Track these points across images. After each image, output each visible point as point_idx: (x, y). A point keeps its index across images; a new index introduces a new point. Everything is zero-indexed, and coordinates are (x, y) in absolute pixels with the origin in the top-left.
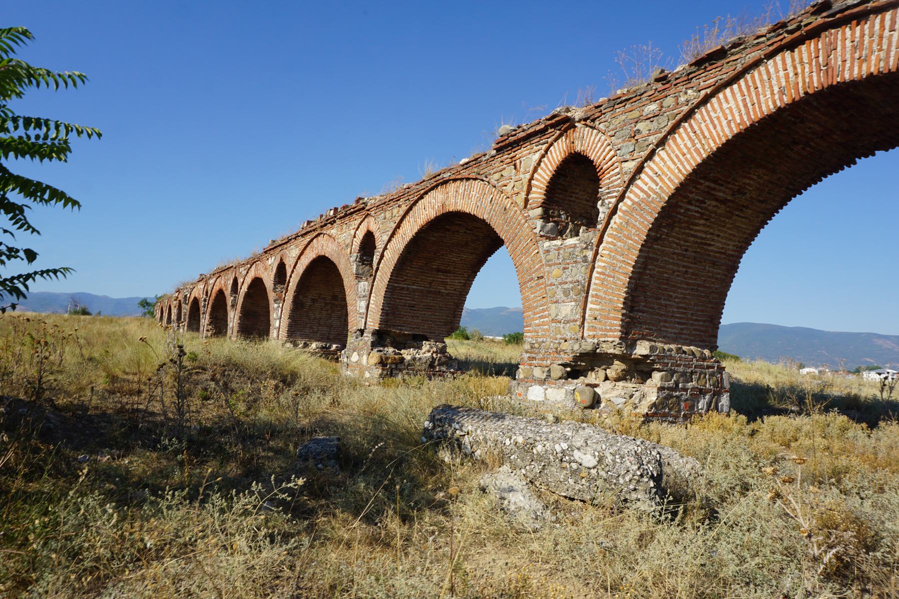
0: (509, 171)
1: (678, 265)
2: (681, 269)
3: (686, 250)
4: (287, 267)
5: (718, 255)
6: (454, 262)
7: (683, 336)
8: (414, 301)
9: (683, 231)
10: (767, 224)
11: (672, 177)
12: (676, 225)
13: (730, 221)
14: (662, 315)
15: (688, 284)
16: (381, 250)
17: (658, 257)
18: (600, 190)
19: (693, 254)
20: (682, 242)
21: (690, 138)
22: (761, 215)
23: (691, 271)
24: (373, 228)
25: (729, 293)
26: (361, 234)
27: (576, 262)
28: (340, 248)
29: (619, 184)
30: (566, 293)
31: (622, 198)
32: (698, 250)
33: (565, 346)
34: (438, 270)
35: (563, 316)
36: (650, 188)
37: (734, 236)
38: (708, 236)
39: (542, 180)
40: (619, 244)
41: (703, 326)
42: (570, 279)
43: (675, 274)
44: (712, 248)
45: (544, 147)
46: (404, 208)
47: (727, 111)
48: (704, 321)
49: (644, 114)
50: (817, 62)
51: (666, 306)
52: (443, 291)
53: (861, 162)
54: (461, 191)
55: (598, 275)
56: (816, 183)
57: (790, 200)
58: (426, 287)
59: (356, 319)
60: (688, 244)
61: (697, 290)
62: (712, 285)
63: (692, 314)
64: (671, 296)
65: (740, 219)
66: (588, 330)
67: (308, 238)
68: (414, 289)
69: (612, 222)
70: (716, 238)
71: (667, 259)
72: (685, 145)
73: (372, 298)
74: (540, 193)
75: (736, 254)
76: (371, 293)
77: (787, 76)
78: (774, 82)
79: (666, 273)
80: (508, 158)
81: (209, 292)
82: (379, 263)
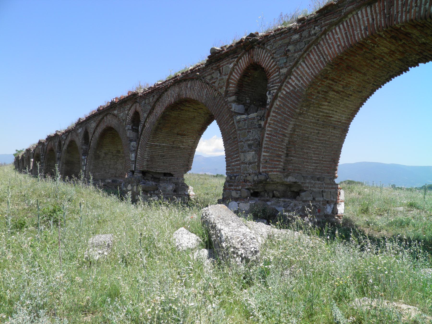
0: (216, 75)
1: (313, 128)
2: (315, 131)
3: (318, 120)
4: (89, 134)
5: (336, 123)
6: (187, 129)
8: (164, 153)
9: (315, 109)
10: (363, 105)
11: (308, 77)
12: (311, 105)
13: (343, 103)
15: (319, 140)
16: (143, 123)
17: (302, 124)
18: (268, 85)
19: (322, 122)
20: (316, 116)
21: (317, 55)
22: (361, 100)
24: (139, 109)
25: (343, 145)
26: (131, 113)
27: (255, 128)
28: (120, 122)
29: (279, 81)
30: (250, 146)
31: (279, 89)
32: (325, 120)
33: (249, 178)
34: (178, 134)
35: (248, 160)
36: (296, 84)
37: (345, 111)
38: (331, 112)
39: (235, 79)
40: (279, 117)
42: (251, 138)
43: (312, 134)
44: (333, 119)
45: (236, 60)
46: (156, 97)
47: (337, 40)
48: (329, 162)
49: (292, 41)
50: (384, 12)
52: (181, 146)
53: (412, 69)
54: (189, 86)
55: (268, 136)
56: (388, 81)
57: (375, 91)
58: (171, 144)
59: (129, 165)
60: (319, 116)
62: (334, 141)
63: (322, 158)
64: (310, 147)
65: (348, 102)
66: (263, 168)
67: (101, 117)
68: (163, 146)
69: (275, 104)
70: (335, 113)
71: (307, 125)
72: (315, 59)
73: (139, 152)
74: (234, 87)
75: (347, 122)
76: (137, 149)
77: (368, 20)
78: (361, 22)
79: (307, 134)
80: (215, 66)
81: (45, 150)
82: (142, 131)
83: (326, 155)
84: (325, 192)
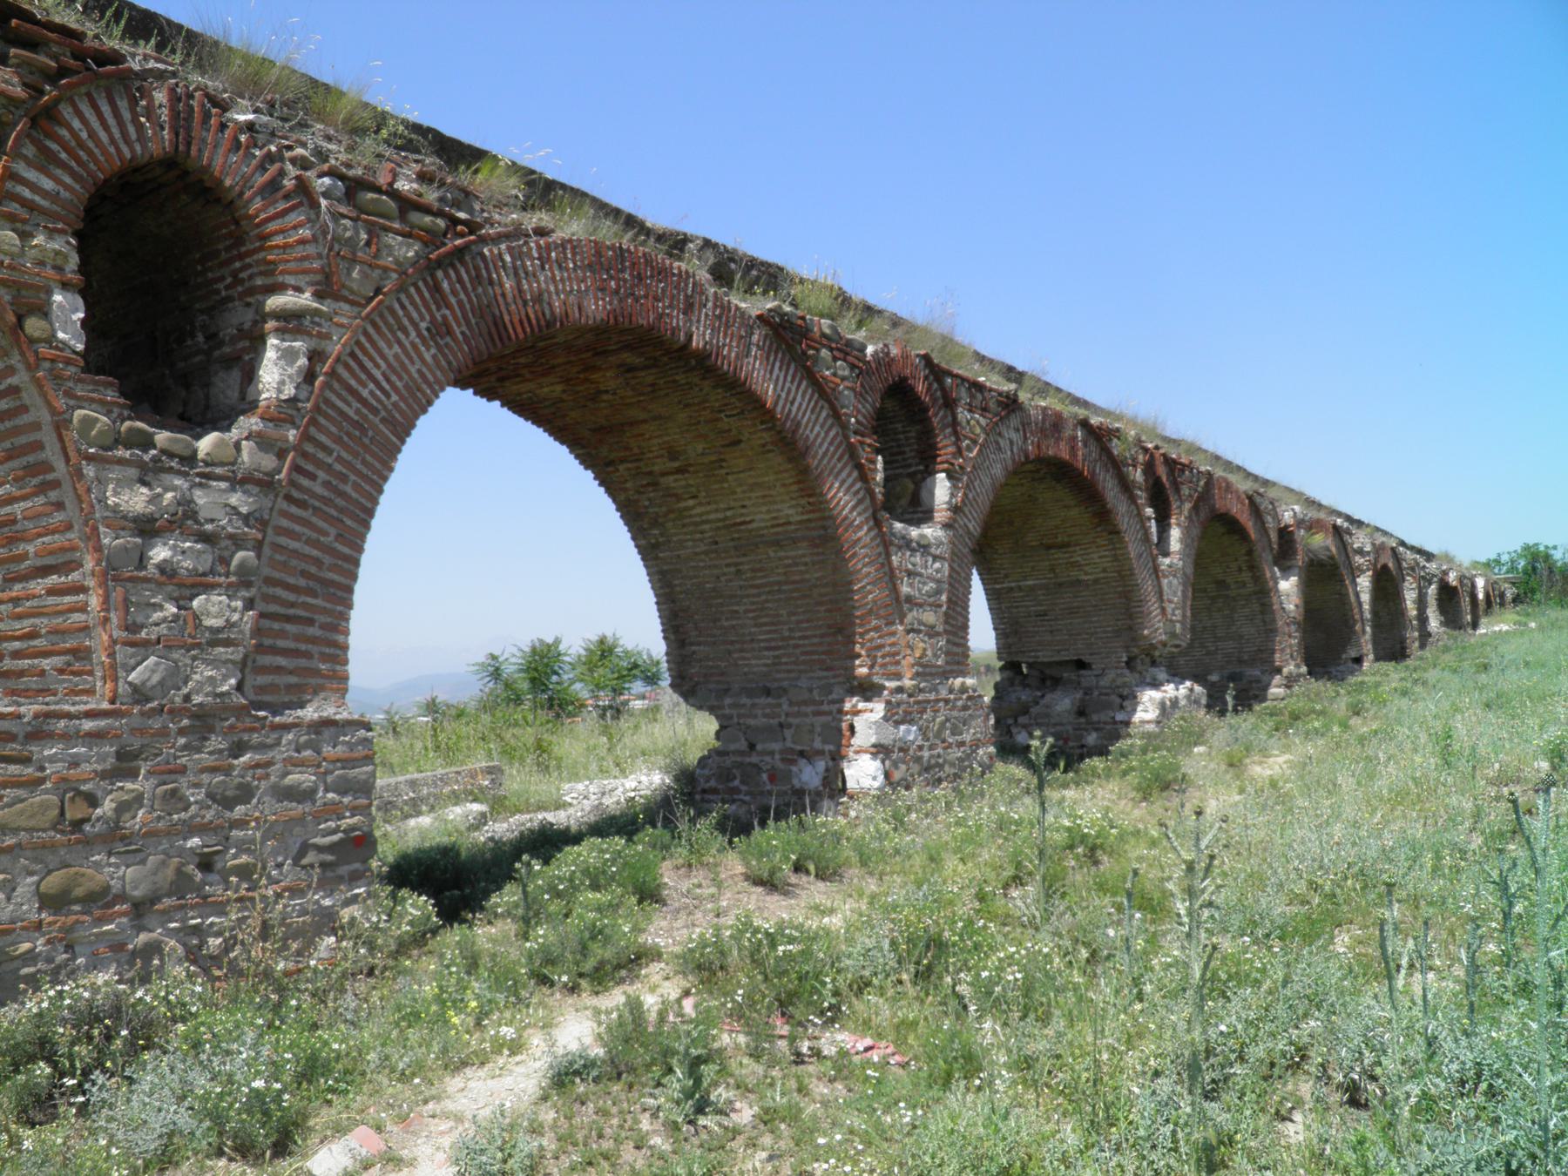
1: (716, 566)
2: (725, 570)
7: (784, 667)
14: (732, 643)
19: (732, 544)
20: (698, 536)
23: (746, 567)
38: (729, 513)
41: (821, 644)
43: (723, 579)
48: (823, 636)
51: (733, 627)
52: (1086, 578)
61: (779, 591)
64: (737, 612)
70: (744, 511)
83: (802, 622)
84: (790, 726)
